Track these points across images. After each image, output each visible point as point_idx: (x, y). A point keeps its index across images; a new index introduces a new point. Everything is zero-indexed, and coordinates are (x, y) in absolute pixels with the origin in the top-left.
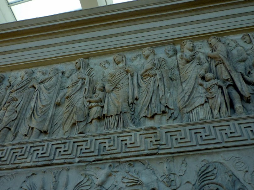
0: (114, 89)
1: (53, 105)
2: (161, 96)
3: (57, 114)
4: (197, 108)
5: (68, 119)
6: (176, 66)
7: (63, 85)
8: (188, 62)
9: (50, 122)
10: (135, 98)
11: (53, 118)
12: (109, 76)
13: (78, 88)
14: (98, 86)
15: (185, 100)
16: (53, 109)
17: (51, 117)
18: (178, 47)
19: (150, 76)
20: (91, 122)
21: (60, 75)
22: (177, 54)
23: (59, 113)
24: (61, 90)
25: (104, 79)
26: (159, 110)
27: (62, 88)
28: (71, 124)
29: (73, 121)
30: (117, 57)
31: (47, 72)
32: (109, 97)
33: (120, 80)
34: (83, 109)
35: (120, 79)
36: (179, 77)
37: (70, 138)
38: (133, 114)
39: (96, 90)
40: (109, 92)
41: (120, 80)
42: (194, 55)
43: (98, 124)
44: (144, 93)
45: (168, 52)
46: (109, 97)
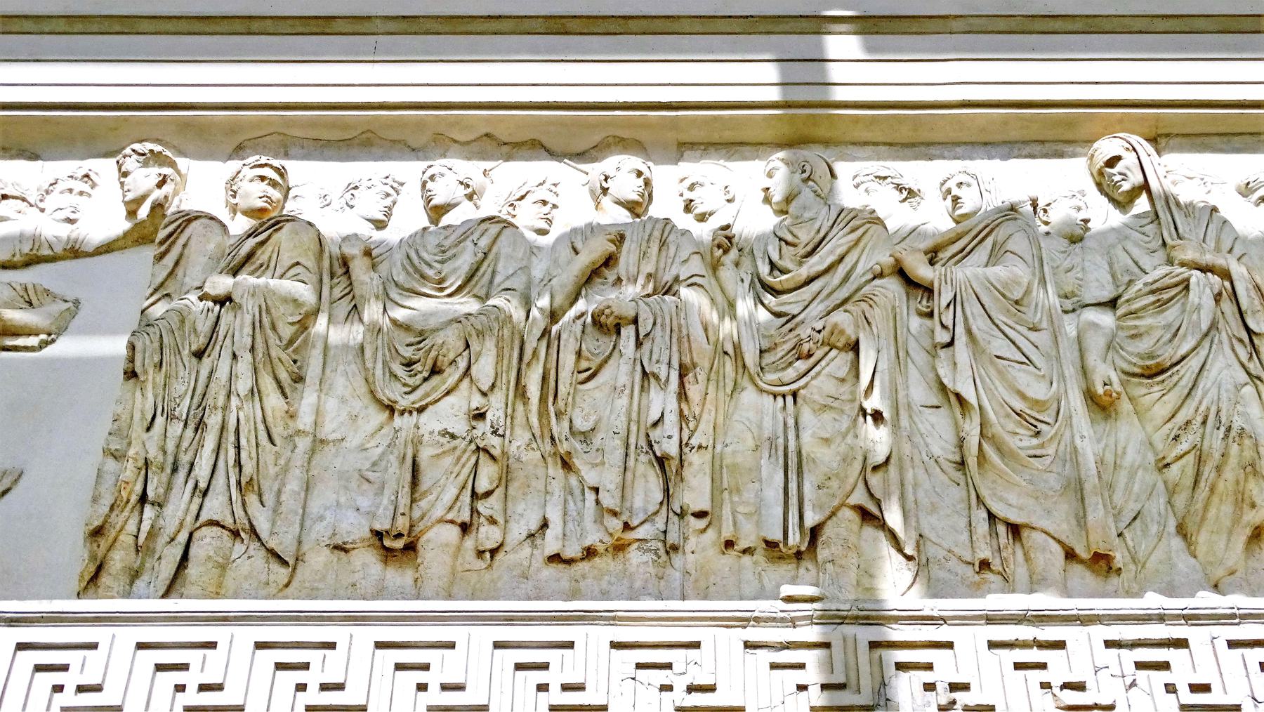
1: (1076, 401)
3: (1109, 458)
5: (1215, 499)
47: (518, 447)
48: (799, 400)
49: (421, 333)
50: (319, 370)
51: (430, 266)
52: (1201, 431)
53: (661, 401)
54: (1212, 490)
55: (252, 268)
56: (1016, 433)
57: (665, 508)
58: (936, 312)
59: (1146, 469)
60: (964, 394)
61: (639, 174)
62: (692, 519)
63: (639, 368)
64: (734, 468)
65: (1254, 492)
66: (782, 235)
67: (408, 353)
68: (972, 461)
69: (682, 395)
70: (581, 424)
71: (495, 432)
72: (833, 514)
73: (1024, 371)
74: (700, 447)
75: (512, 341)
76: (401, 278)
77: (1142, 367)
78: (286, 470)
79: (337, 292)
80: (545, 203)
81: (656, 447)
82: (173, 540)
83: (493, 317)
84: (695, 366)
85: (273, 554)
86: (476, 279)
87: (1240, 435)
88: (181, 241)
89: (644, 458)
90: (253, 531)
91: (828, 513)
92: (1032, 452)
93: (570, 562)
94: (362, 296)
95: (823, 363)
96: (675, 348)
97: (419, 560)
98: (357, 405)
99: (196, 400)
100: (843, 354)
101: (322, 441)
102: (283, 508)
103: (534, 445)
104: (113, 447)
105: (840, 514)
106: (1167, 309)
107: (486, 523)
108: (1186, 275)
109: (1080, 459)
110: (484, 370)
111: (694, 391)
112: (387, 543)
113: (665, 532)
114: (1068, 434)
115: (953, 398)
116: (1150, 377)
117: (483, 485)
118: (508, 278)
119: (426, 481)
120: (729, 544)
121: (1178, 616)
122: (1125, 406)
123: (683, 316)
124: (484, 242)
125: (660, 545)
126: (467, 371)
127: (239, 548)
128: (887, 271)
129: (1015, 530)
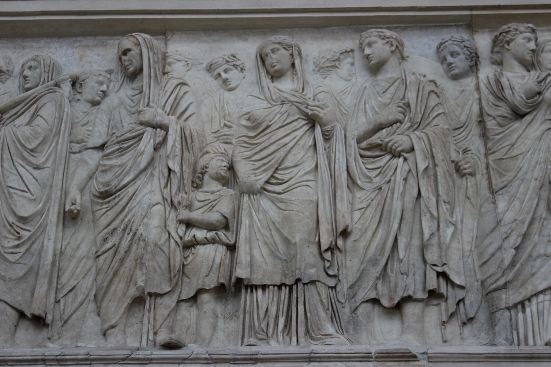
0: (267, 182)
1: (53, 215)
2: (426, 236)
3: (69, 251)
4: (541, 297)
5: (117, 279)
6: (475, 118)
7: (81, 132)
8: (518, 115)
9: (50, 283)
10: (340, 229)
11: (59, 266)
12: (244, 122)
13: (144, 161)
14: (216, 165)
15: (502, 261)
16: (57, 231)
17: (53, 263)
18: (483, 41)
19: (391, 152)
20: (194, 299)
21: (66, 94)
22: (477, 70)
23: (78, 247)
24: (74, 153)
25: (226, 131)
26: (420, 286)
27: (76, 147)
28: (128, 301)
29: (133, 292)
30: (273, 51)
31: (10, 68)
32: (254, 214)
33: (289, 152)
34: (165, 249)
35: (288, 147)
36: (484, 166)
37: (138, 359)
38: (332, 288)
39: (206, 177)
40: (251, 192)
41: (289, 152)
42: (539, 93)
43: (219, 309)
44: (369, 210)
45: (450, 59)
46: (253, 212)
52: (121, 235)
54: (115, 274)
56: (7, 238)
65: (139, 275)
77: (99, 192)
92: (11, 250)
106: (125, 154)
108: (140, 132)
109: (43, 254)
116: (104, 199)
122: (89, 217)
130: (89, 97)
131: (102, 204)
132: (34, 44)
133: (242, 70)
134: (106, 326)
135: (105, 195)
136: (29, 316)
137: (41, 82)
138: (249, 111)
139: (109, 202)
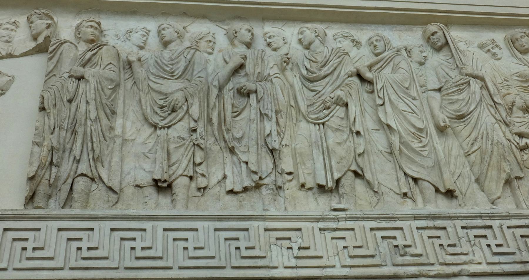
5: (490, 168)
25: (506, 83)
28: (503, 181)
29: (504, 176)
39: (515, 108)
47: (210, 144)
48: (325, 126)
49: (166, 94)
50: (122, 109)
51: (167, 66)
53: (269, 126)
55: (91, 65)
57: (274, 171)
58: (376, 91)
59: (460, 156)
60: (391, 125)
61: (249, 31)
62: (286, 175)
63: (259, 111)
64: (301, 154)
66: (310, 58)
67: (161, 103)
68: (397, 152)
69: (278, 123)
70: (238, 135)
71: (201, 138)
72: (345, 174)
73: (413, 116)
74: (286, 145)
75: (204, 99)
76: (154, 71)
78: (112, 152)
79: (127, 76)
80: (210, 41)
81: (269, 145)
82: (65, 182)
83: (196, 88)
84: (281, 111)
85: (110, 188)
86: (186, 72)
87: (497, 143)
88: (59, 52)
89: (264, 150)
90: (100, 178)
91: (342, 173)
93: (237, 193)
94: (138, 78)
95: (335, 111)
96: (273, 104)
97: (173, 192)
98: (139, 125)
99: (70, 121)
100: (341, 108)
101: (126, 140)
102: (113, 169)
103: (216, 143)
104: (37, 141)
105: (347, 174)
107: (200, 176)
108: (468, 79)
109: (437, 152)
110: (195, 110)
111: (281, 121)
112: (160, 184)
113: (275, 181)
114: (431, 142)
115: (386, 127)
116: (459, 119)
117: (198, 160)
118: (199, 72)
119: (173, 159)
120: (303, 186)
121: (487, 216)
123: (274, 90)
124: (189, 57)
125: (274, 186)
126: (187, 111)
127: (94, 186)
128: (353, 75)
129: (415, 180)
130: (418, 60)
131: (460, 123)
132: (368, 28)
133: (500, 48)
134: (495, 197)
135: (460, 117)
136: (443, 190)
137: (387, 49)
138: (517, 72)
139: (464, 121)
